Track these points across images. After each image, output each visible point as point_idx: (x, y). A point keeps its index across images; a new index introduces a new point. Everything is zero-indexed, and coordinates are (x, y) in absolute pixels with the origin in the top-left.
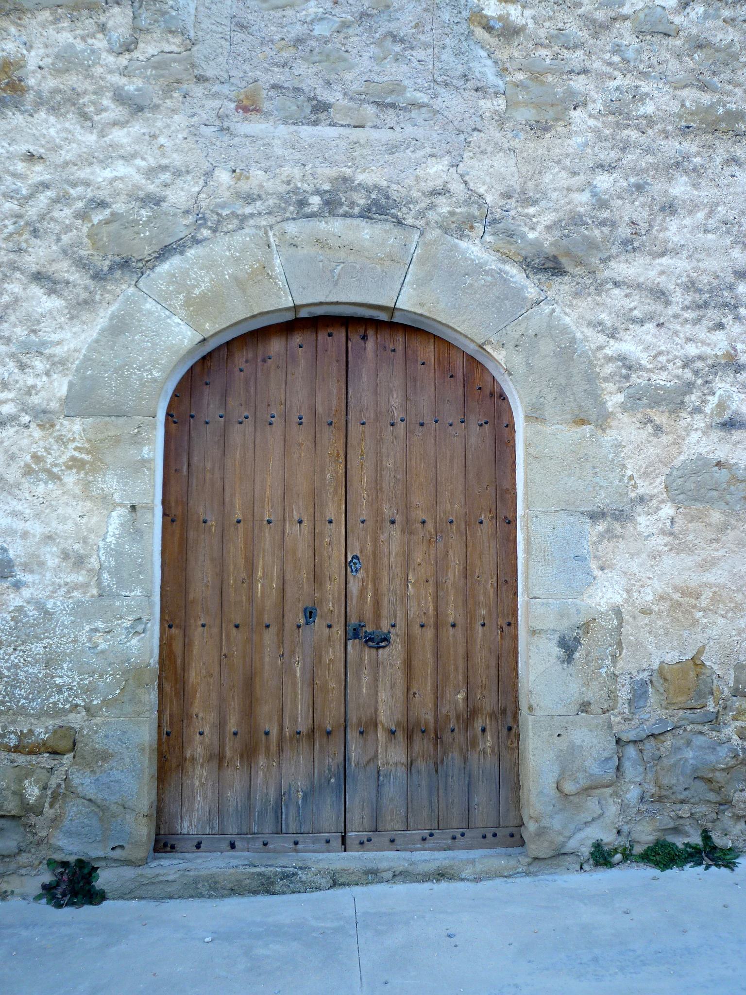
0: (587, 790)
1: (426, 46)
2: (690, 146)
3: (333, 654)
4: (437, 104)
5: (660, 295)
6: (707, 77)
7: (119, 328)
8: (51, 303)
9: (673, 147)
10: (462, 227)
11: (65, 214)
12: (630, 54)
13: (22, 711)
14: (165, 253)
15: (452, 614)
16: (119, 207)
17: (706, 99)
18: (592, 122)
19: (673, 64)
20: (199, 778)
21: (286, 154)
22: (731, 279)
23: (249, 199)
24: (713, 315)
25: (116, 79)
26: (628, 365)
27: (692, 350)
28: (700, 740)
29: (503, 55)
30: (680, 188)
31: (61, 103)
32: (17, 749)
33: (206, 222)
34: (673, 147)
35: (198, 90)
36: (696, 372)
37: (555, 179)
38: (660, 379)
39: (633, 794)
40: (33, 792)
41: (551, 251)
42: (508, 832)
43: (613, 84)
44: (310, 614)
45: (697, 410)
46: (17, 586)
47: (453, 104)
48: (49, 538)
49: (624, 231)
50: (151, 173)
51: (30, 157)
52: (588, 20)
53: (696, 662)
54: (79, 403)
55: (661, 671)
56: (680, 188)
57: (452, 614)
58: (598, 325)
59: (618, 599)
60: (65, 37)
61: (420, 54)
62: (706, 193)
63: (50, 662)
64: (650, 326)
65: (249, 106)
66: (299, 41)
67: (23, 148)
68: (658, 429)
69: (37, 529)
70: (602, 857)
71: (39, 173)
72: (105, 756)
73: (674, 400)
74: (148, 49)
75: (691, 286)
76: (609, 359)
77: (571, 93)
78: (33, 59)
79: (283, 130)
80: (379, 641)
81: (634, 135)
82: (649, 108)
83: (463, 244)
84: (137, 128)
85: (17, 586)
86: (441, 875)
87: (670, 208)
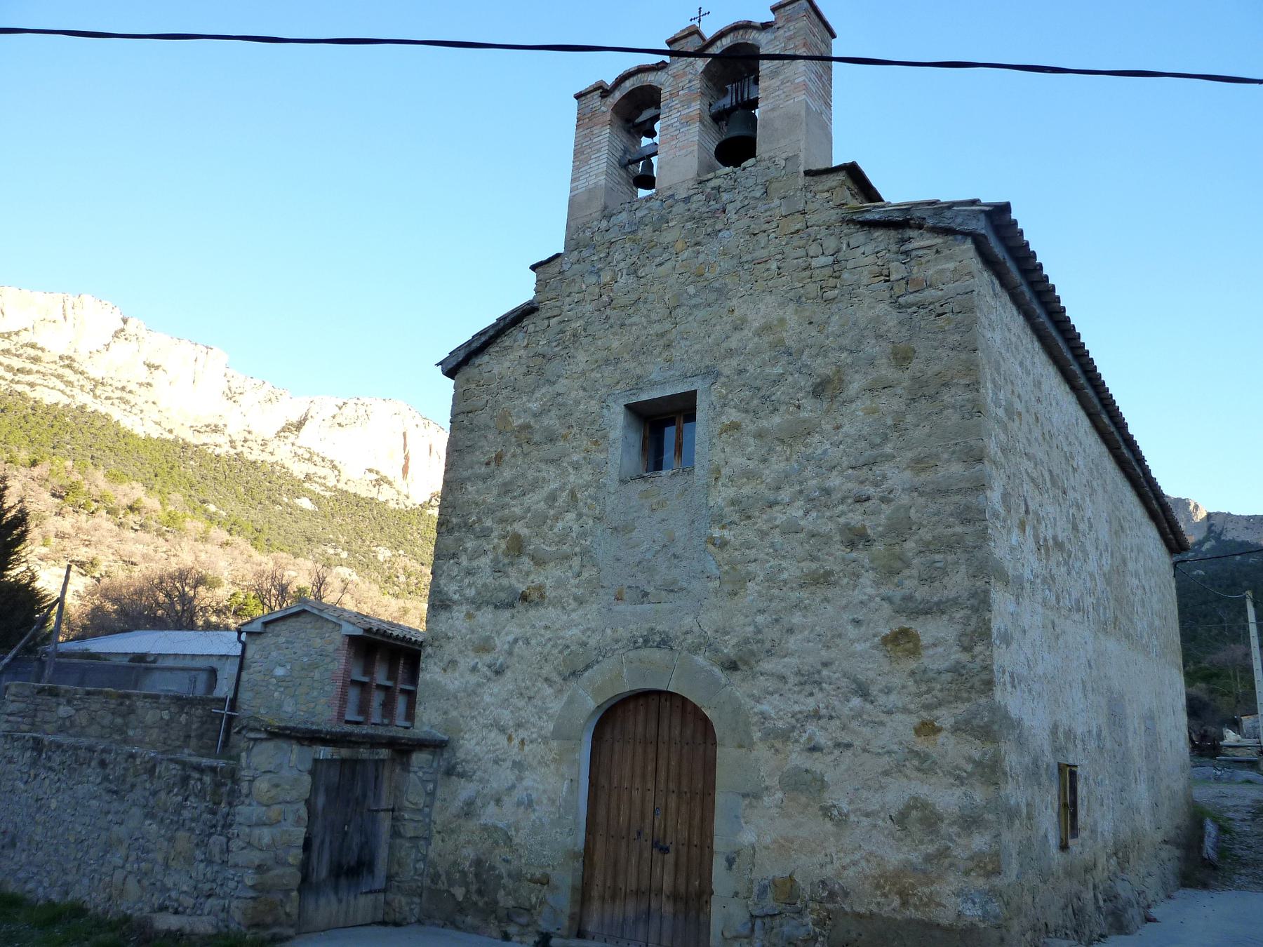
0: (736, 938)
1: (687, 558)
2: (804, 594)
3: (647, 854)
5: (783, 678)
6: (815, 553)
7: (570, 701)
9: (794, 595)
10: (695, 649)
11: (555, 652)
12: (778, 547)
13: (532, 864)
14: (587, 667)
15: (696, 841)
16: (573, 648)
17: (814, 566)
18: (757, 588)
19: (799, 549)
20: (596, 905)
22: (819, 667)
23: (617, 641)
24: (808, 688)
25: (574, 590)
26: (764, 716)
27: (797, 708)
28: (794, 923)
29: (719, 558)
30: (797, 619)
31: (558, 603)
32: (530, 881)
33: (602, 652)
34: (794, 595)
35: (601, 592)
36: (797, 720)
38: (780, 724)
40: (534, 900)
41: (734, 658)
43: (768, 565)
44: (639, 833)
45: (797, 741)
46: (534, 810)
47: (696, 586)
48: (545, 791)
49: (768, 645)
50: (584, 632)
51: (546, 627)
54: (557, 734)
55: (773, 881)
56: (797, 619)
57: (696, 841)
58: (752, 696)
59: (753, 840)
60: (558, 573)
61: (684, 563)
62: (811, 619)
63: (542, 844)
64: (776, 696)
65: (619, 598)
67: (543, 624)
68: (777, 750)
69: (541, 787)
71: (548, 634)
72: (557, 888)
73: (785, 735)
74: (585, 575)
75: (799, 673)
76: (756, 714)
77: (748, 573)
78: (548, 583)
79: (631, 608)
80: (665, 850)
81: (775, 592)
82: (785, 575)
83: (696, 658)
84: (581, 612)
85: (534, 810)
87: (790, 631)
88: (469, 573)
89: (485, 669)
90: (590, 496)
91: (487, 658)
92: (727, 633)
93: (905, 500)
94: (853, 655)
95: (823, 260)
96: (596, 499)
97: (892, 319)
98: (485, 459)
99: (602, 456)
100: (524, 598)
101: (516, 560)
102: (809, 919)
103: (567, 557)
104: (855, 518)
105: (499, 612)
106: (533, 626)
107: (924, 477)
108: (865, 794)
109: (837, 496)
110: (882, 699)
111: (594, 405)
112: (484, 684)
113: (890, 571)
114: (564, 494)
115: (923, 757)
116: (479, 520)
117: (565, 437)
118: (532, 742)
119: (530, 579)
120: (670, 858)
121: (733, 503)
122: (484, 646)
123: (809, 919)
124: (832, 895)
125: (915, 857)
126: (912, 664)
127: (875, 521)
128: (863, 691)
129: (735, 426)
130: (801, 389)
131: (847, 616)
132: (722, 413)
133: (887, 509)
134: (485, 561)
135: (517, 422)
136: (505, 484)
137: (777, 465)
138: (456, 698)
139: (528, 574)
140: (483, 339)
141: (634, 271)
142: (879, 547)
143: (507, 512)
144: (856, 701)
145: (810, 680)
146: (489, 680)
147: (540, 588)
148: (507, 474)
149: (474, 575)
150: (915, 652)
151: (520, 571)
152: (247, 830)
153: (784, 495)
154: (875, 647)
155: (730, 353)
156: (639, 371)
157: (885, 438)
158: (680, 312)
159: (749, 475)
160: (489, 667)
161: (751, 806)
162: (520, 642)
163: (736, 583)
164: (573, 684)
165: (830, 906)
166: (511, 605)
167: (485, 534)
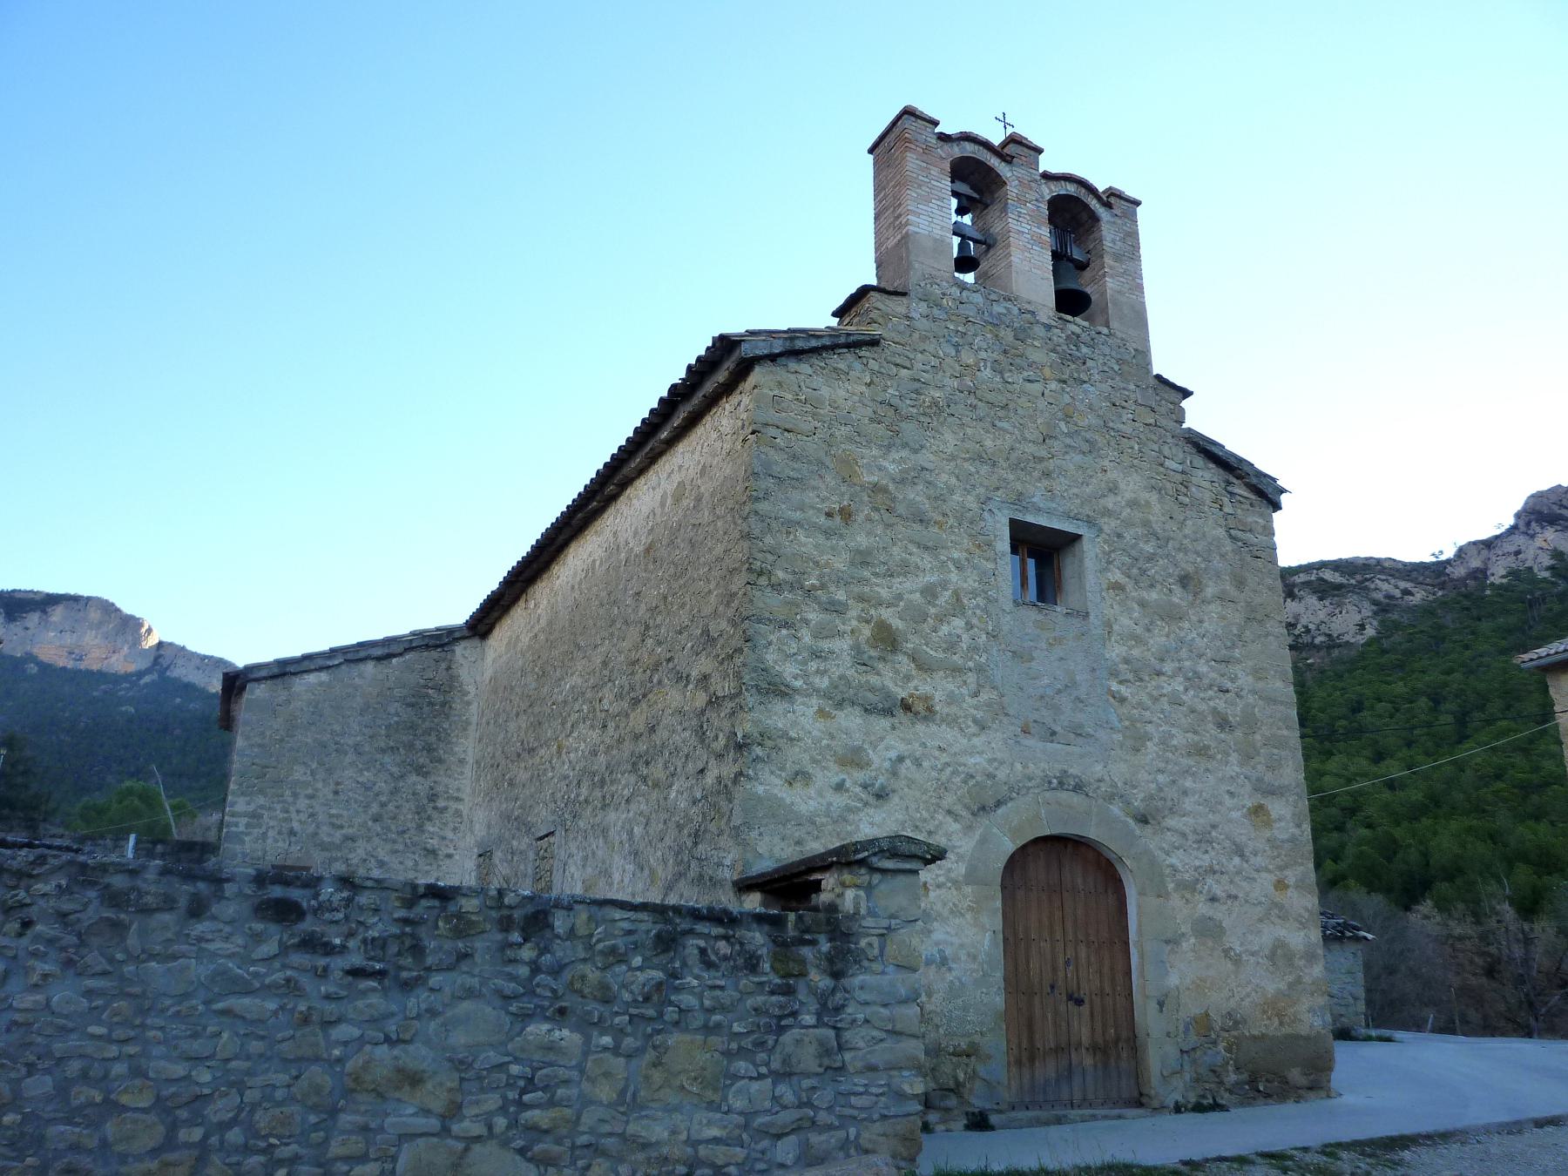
4: (1097, 735)
5: (1184, 835)
7: (983, 841)
8: (956, 826)
9: (1185, 761)
10: (1110, 798)
14: (999, 804)
15: (1108, 989)
16: (979, 778)
21: (1043, 758)
23: (1030, 779)
24: (1204, 845)
27: (1197, 863)
30: (1189, 783)
31: (951, 721)
32: (953, 1054)
33: (1015, 790)
35: (1005, 720)
37: (1143, 776)
38: (1186, 876)
39: (1187, 1077)
40: (961, 1076)
42: (1139, 1101)
44: (1052, 987)
46: (950, 969)
47: (1102, 735)
48: (962, 946)
49: (1169, 803)
50: (991, 761)
52: (1150, 695)
53: (1207, 1015)
57: (1108, 989)
58: (1162, 849)
60: (951, 687)
63: (965, 1009)
65: (1025, 731)
66: (1042, 697)
69: (956, 940)
70: (1178, 1109)
72: (989, 1057)
74: (984, 697)
75: (1195, 832)
78: (938, 696)
79: (1040, 745)
80: (1079, 1002)
82: (1175, 742)
84: (983, 738)
85: (950, 969)
86: (1119, 1117)
87: (1185, 793)
88: (816, 655)
89: (858, 789)
90: (978, 606)
91: (860, 776)
92: (1135, 787)
93: (1251, 699)
94: (1230, 821)
95: (1174, 465)
96: (986, 610)
97: (1228, 546)
98: (825, 506)
99: (990, 566)
100: (906, 707)
101: (890, 657)
102: (1221, 1046)
103: (956, 670)
104: (1220, 704)
105: (872, 718)
106: (924, 745)
107: (1260, 685)
108: (1250, 937)
109: (1206, 681)
110: (1253, 860)
111: (971, 502)
112: (859, 809)
113: (1248, 757)
114: (948, 593)
115: (1280, 907)
116: (823, 587)
117: (940, 525)
118: (939, 886)
119: (911, 685)
120: (1085, 1009)
121: (1126, 661)
122: (853, 759)
123: (1221, 1046)
124: (1236, 1023)
125: (1283, 986)
126: (1268, 834)
127: (1234, 713)
128: (1239, 851)
129: (1117, 587)
130: (1170, 575)
131: (1224, 788)
132: (1106, 570)
133: (1241, 704)
134: (842, 645)
135: (870, 478)
136: (859, 552)
137: (1158, 640)
138: (814, 823)
139: (908, 678)
140: (814, 343)
141: (997, 369)
142: (1239, 733)
143: (867, 589)
144: (1237, 860)
145: (1204, 839)
146: (866, 804)
147: (926, 698)
148: (862, 541)
149: (826, 659)
150: (1268, 824)
151: (897, 672)
152: (885, 1012)
153: (1168, 667)
154: (1244, 816)
155: (1107, 513)
156: (1019, 486)
157: (1234, 646)
158: (1057, 445)
159: (1138, 640)
160: (865, 787)
161: (1172, 951)
162: (908, 762)
163: (1137, 742)
164: (984, 821)
165: (1235, 1033)
166: (888, 712)
167: (835, 608)
